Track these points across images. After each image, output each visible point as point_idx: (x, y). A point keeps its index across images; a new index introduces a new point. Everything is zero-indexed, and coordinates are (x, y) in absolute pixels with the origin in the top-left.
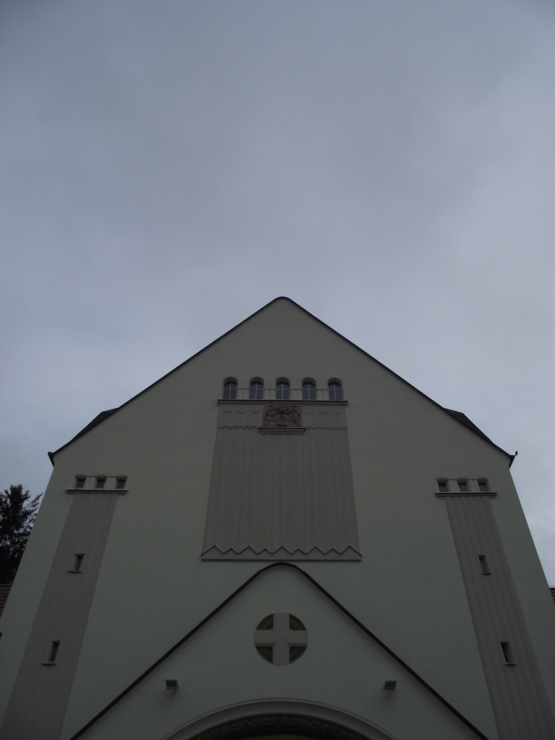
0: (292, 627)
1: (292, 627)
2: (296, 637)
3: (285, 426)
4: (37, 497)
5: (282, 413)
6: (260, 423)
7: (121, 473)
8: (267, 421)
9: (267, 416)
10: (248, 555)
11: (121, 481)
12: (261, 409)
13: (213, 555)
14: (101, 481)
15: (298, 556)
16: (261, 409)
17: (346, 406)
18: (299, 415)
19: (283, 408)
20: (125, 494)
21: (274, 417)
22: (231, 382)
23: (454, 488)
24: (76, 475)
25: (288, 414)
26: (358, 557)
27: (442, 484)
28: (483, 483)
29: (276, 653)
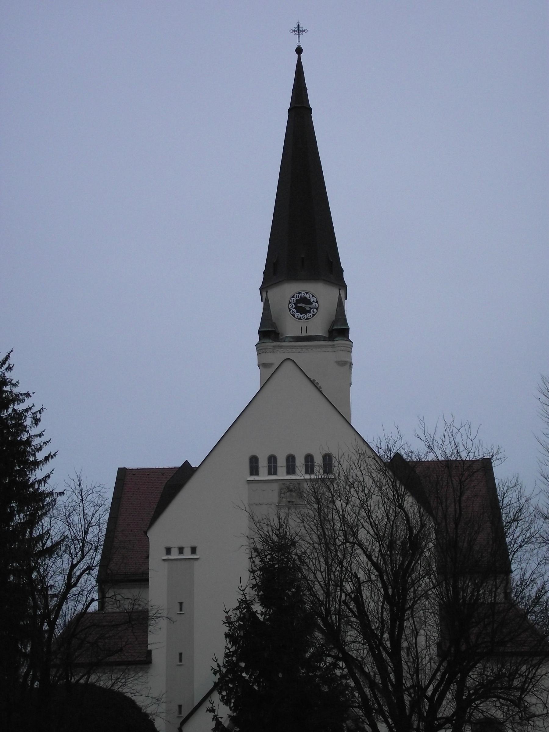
3: (293, 502)
4: (7, 354)
5: (291, 491)
7: (194, 545)
8: (281, 498)
9: (281, 493)
11: (194, 550)
12: (276, 487)
14: (181, 550)
20: (198, 560)
21: (286, 494)
22: (254, 461)
24: (165, 547)
25: (295, 492)
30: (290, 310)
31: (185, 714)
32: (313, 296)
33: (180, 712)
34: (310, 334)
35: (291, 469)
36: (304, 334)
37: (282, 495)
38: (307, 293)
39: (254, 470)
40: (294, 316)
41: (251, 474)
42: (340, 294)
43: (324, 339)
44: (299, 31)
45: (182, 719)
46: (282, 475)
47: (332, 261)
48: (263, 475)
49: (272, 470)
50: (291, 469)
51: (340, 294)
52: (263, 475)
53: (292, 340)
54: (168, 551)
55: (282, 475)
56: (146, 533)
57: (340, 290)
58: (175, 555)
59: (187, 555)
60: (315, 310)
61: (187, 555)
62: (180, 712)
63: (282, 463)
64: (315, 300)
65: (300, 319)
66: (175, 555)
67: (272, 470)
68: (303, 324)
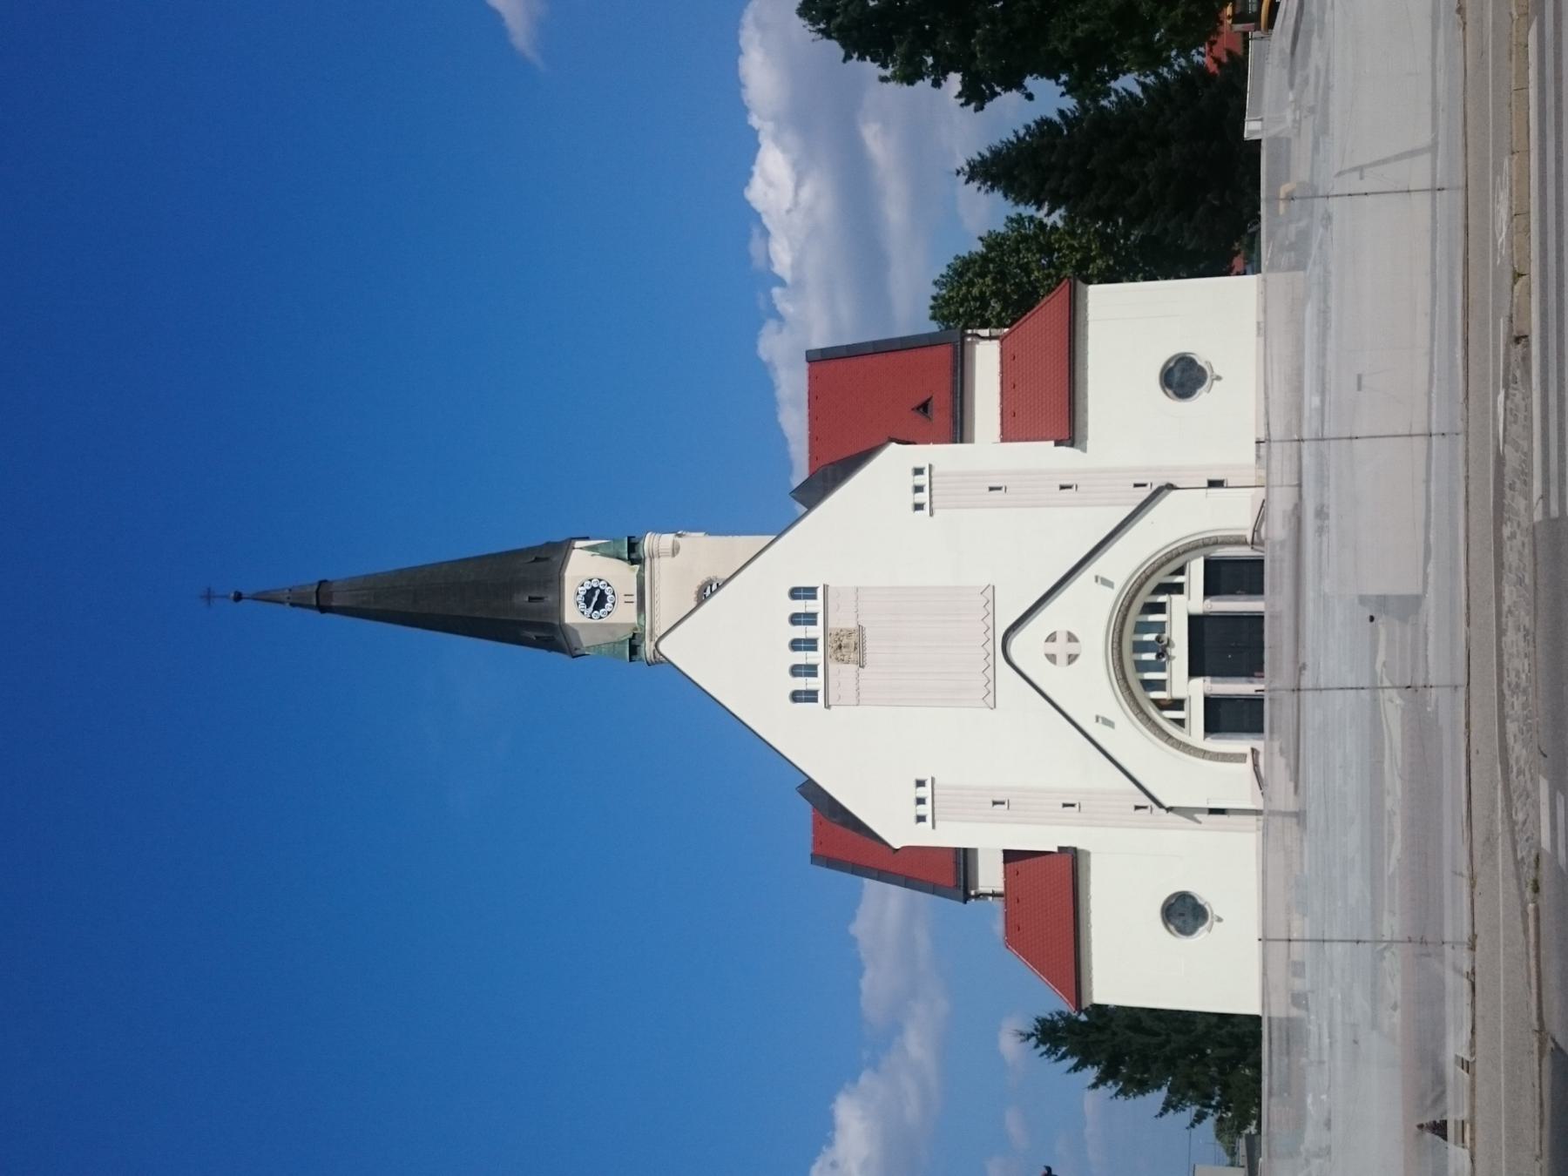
0: (1054, 640)
1: (1054, 640)
2: (1062, 638)
3: (856, 644)
6: (853, 667)
7: (913, 784)
10: (990, 672)
11: (920, 783)
12: (834, 667)
13: (990, 699)
14: (920, 801)
15: (990, 633)
16: (834, 667)
17: (828, 586)
18: (841, 631)
19: (834, 645)
22: (796, 697)
23: (923, 497)
24: (914, 823)
26: (991, 588)
27: (918, 507)
28: (918, 471)
29: (1073, 652)
30: (601, 618)
31: (1147, 802)
32: (582, 585)
33: (1145, 807)
34: (634, 591)
35: (810, 644)
36: (635, 599)
37: (846, 658)
38: (578, 594)
39: (810, 696)
40: (609, 613)
41: (815, 700)
42: (581, 548)
43: (642, 571)
44: (209, 596)
45: (1154, 805)
46: (815, 657)
47: (533, 559)
48: (815, 683)
49: (810, 670)
50: (810, 644)
51: (581, 548)
52: (815, 683)
53: (643, 616)
54: (921, 819)
55: (815, 657)
56: (897, 850)
57: (574, 548)
58: (925, 810)
59: (925, 792)
60: (602, 583)
61: (925, 792)
62: (1145, 807)
63: (802, 658)
64: (589, 582)
65: (613, 604)
66: (925, 810)
67: (810, 670)
68: (621, 599)
